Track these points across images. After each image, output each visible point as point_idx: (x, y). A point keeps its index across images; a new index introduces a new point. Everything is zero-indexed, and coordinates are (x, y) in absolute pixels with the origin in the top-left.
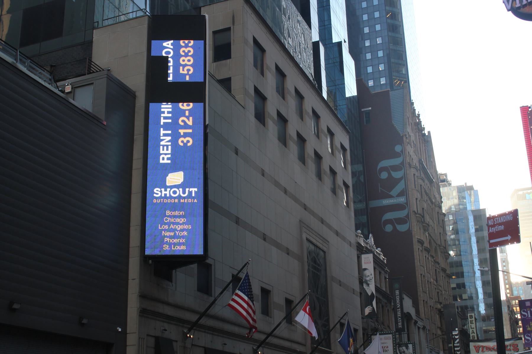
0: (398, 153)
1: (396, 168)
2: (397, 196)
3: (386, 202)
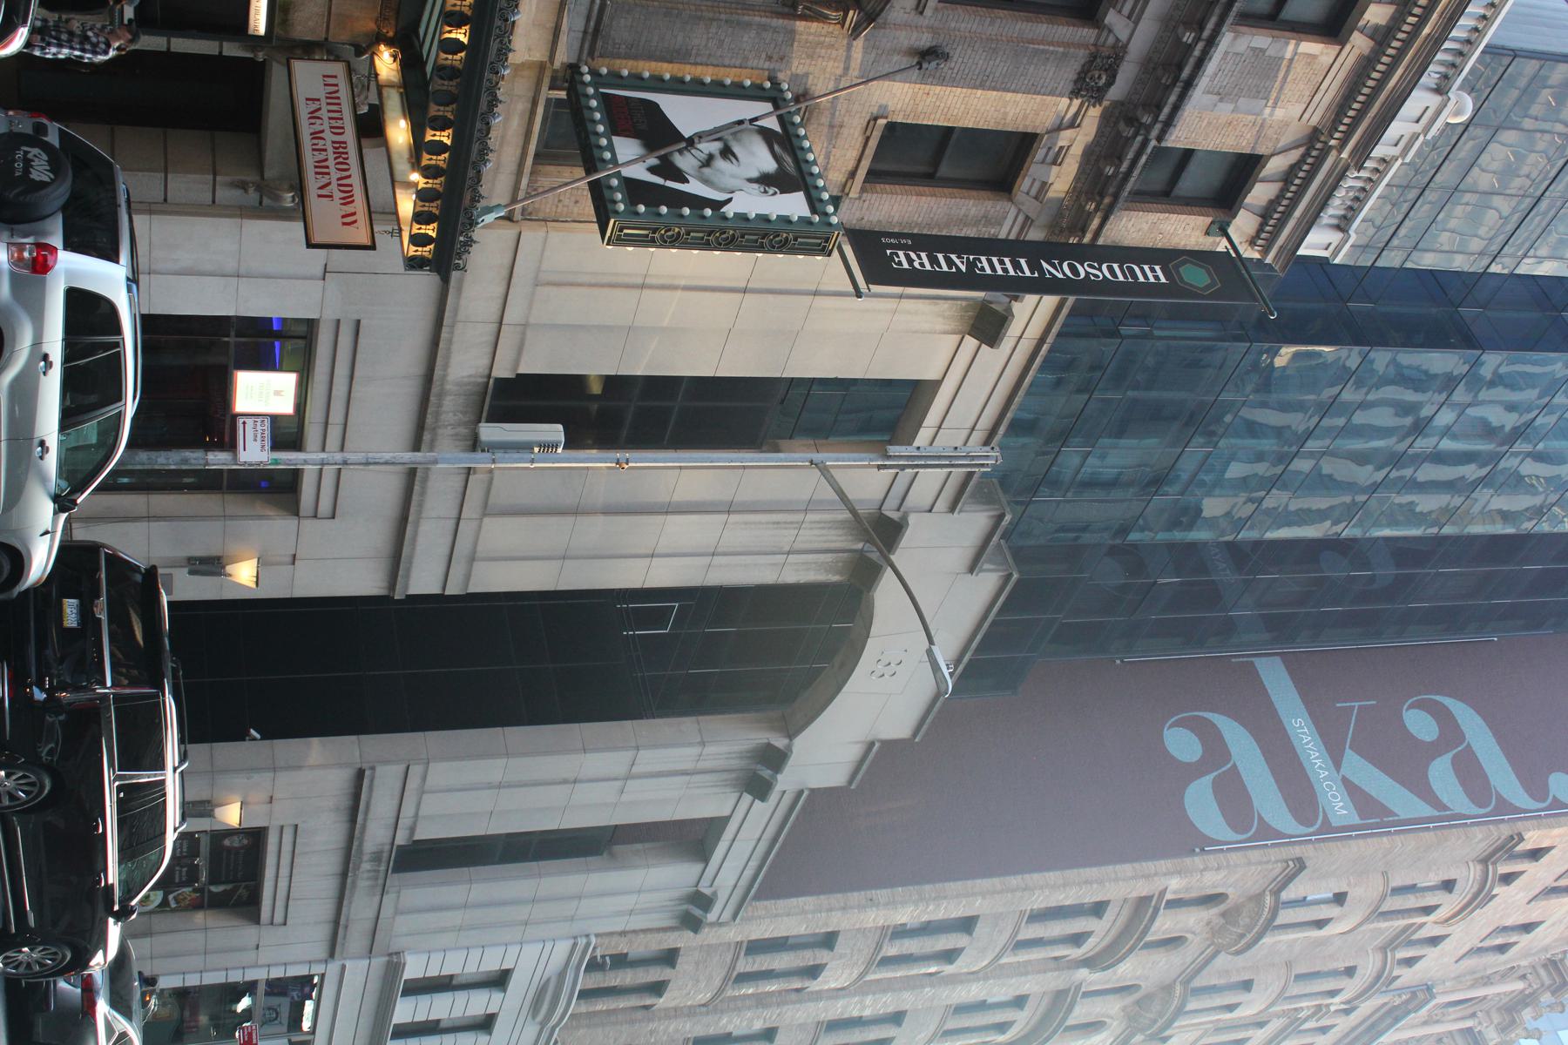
0: (1546, 785)
1: (1470, 773)
2: (1345, 781)
3: (1302, 731)
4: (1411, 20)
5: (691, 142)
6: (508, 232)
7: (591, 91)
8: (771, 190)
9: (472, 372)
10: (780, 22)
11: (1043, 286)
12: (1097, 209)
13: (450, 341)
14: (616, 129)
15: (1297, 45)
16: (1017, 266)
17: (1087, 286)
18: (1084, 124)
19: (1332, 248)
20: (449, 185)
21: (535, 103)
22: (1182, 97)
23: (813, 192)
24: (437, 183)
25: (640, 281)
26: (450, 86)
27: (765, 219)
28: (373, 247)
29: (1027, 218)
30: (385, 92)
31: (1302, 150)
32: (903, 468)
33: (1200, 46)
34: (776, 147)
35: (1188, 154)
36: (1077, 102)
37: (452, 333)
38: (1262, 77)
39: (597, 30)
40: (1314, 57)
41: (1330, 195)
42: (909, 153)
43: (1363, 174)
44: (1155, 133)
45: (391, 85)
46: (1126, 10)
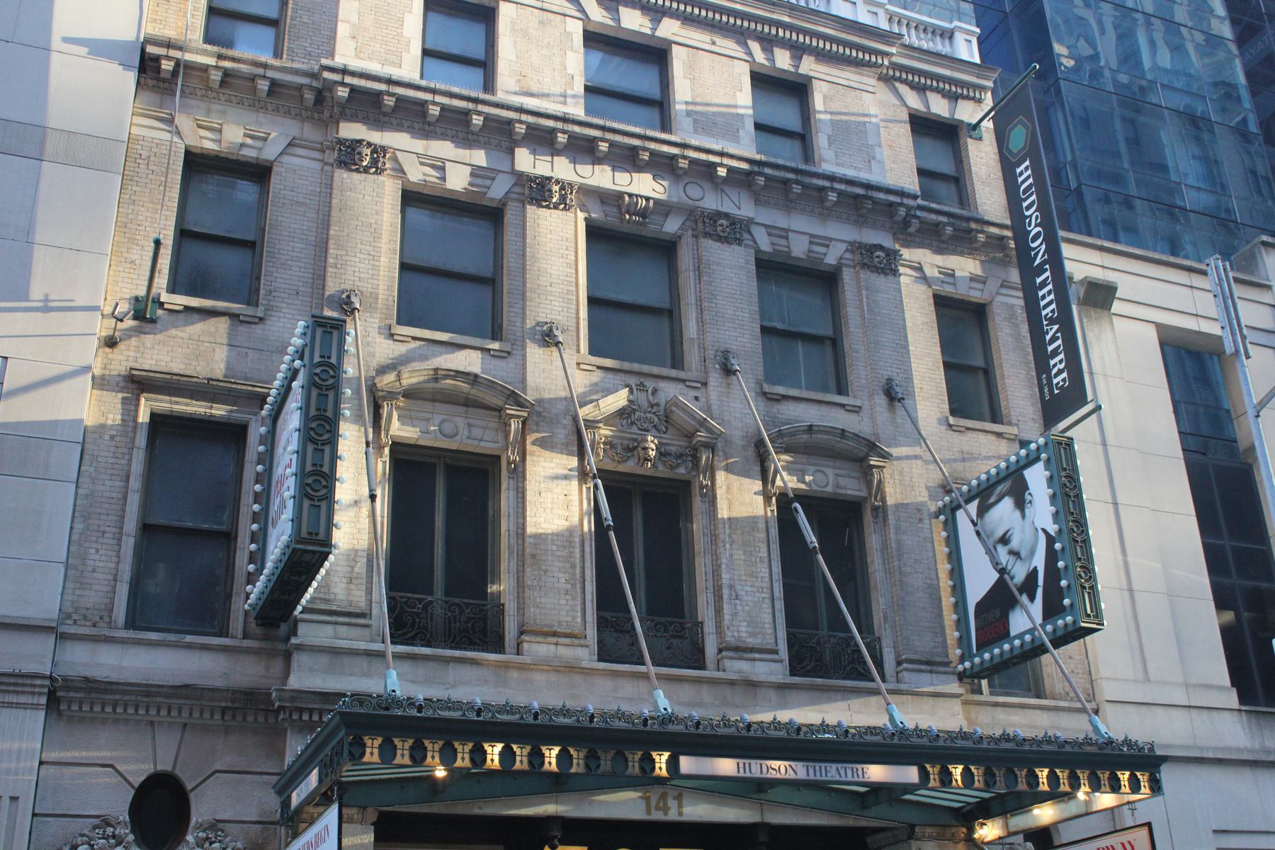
4: (781, 33)
5: (1002, 571)
6: (1108, 710)
7: (977, 660)
8: (1028, 497)
9: (1238, 727)
10: (891, 519)
11: (1055, 259)
12: (982, 232)
13: (1215, 749)
14: (1005, 635)
15: (819, 112)
16: (1044, 284)
17: (1046, 223)
18: (916, 259)
19: (969, 38)
20: (1083, 766)
21: (996, 705)
22: (879, 189)
23: (1022, 463)
24: (1083, 776)
25: (1126, 594)
26: (1000, 774)
27: (1053, 498)
28: (1149, 825)
29: (1002, 286)
30: (1012, 829)
31: (897, 85)
32: (1244, 338)
33: (837, 186)
34: (992, 500)
35: (922, 172)
36: (902, 270)
37: (1207, 748)
38: (852, 132)
39: (928, 663)
40: (825, 97)
41: (928, 52)
42: (972, 393)
43: (904, 31)
44: (911, 202)
45: (1006, 825)
46: (823, 250)
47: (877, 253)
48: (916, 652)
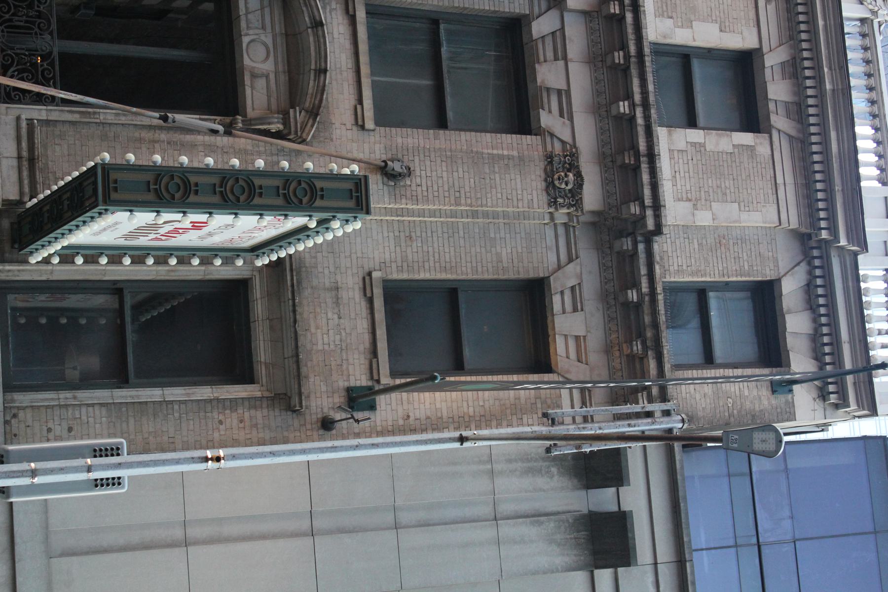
12: (645, 347)
29: (577, 338)
31: (803, 267)
33: (639, 112)
47: (571, 175)
48: (45, 147)
